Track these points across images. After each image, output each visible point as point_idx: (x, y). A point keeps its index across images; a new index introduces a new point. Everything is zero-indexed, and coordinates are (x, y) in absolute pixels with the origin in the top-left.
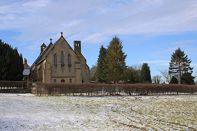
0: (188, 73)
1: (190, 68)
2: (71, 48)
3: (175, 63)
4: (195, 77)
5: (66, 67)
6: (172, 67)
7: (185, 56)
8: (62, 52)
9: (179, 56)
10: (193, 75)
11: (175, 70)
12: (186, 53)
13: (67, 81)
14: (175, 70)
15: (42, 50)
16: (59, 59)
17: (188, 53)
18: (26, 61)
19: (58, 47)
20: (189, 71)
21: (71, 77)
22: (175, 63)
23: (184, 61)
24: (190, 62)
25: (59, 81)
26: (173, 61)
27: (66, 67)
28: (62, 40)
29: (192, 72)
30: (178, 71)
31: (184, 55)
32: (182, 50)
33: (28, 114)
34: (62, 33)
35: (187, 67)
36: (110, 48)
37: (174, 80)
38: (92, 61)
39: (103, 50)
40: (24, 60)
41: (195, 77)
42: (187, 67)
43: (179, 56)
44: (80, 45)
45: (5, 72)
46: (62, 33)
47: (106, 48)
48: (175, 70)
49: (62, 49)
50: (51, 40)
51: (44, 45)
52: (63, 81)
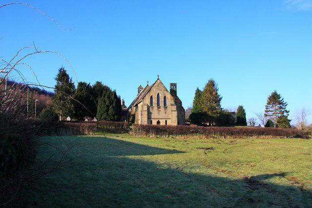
0: (284, 116)
1: (286, 111)
2: (167, 90)
3: (271, 106)
4: (290, 121)
5: (162, 109)
6: (268, 110)
7: (281, 99)
8: (158, 94)
9: (275, 98)
10: (289, 118)
11: (271, 112)
12: (282, 96)
13: (162, 123)
14: (271, 113)
15: (139, 92)
16: (155, 101)
17: (284, 96)
18: (124, 102)
19: (154, 89)
20: (285, 114)
21: (167, 119)
22: (271, 106)
23: (280, 104)
24: (286, 105)
25: (154, 123)
26: (269, 103)
27: (162, 109)
28: (158, 83)
29: (288, 115)
30: (273, 114)
31: (280, 98)
32: (278, 93)
33: (147, 156)
34: (158, 76)
35: (283, 110)
36: (206, 90)
37: (269, 124)
38: (188, 103)
39: (198, 91)
40: (122, 101)
41: (290, 121)
42: (283, 110)
43: (275, 98)
44: (176, 87)
45: (105, 112)
46: (158, 76)
47: (202, 89)
48: (271, 113)
49: (158, 92)
50: (148, 82)
51: (140, 88)
52: (158, 122)
